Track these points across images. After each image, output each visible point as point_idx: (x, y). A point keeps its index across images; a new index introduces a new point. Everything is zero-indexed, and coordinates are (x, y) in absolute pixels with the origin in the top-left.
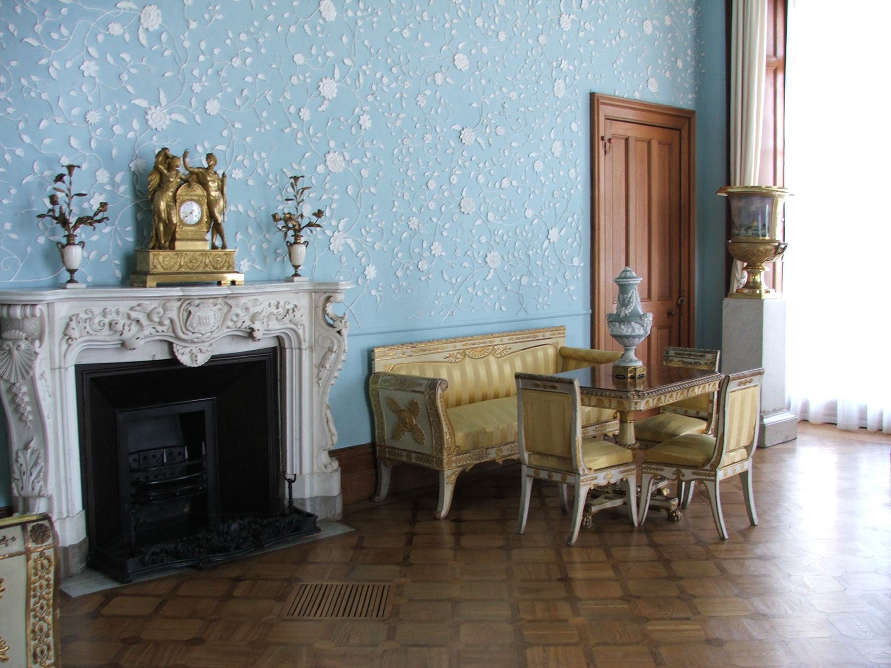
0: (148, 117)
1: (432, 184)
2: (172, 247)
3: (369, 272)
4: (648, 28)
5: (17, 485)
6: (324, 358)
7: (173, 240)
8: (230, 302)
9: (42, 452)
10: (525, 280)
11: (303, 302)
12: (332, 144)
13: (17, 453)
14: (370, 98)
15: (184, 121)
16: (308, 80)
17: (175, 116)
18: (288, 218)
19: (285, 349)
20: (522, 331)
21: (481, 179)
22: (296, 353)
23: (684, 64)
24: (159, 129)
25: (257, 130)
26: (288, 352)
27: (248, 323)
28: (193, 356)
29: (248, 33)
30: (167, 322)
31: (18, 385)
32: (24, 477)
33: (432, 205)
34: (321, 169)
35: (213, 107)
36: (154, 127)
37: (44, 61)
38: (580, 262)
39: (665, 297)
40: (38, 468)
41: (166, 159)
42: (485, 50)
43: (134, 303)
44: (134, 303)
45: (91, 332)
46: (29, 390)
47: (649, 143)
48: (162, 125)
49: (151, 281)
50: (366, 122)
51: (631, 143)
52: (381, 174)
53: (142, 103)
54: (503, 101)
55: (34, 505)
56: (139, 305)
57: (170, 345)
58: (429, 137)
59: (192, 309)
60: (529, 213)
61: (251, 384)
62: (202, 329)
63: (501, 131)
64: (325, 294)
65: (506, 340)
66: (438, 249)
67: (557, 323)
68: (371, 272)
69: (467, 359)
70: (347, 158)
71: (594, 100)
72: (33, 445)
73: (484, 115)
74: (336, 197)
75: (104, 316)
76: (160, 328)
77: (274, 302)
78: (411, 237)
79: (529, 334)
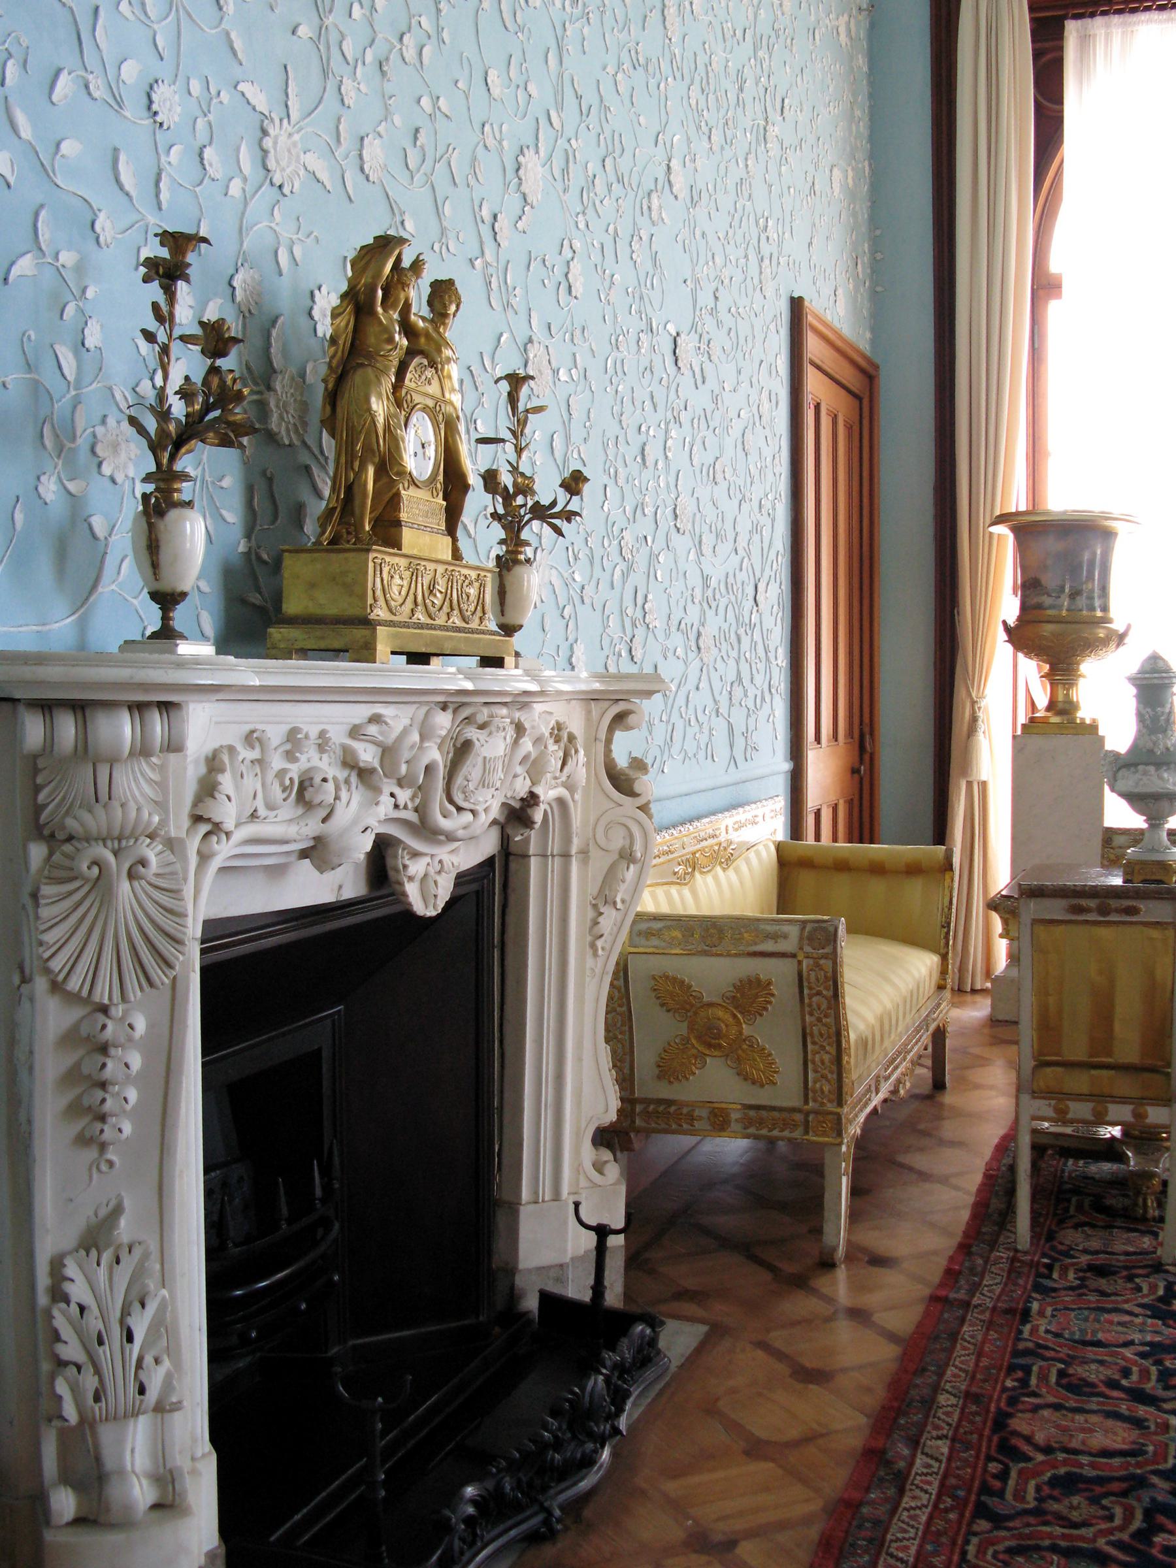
0: (268, 143)
3: (578, 659)
5: (75, 1389)
9: (153, 1246)
13: (57, 1265)
15: (323, 176)
16: (505, 143)
17: (314, 161)
19: (526, 856)
24: (286, 190)
25: (436, 247)
26: (534, 863)
31: (118, 1011)
32: (103, 1353)
36: (277, 180)
38: (782, 659)
39: (850, 733)
40: (152, 1307)
43: (359, 713)
44: (359, 713)
45: (262, 812)
46: (151, 1026)
49: (384, 642)
52: (592, 416)
54: (714, 285)
55: (121, 1442)
56: (375, 719)
59: (472, 733)
69: (697, 874)
70: (554, 365)
72: (125, 1229)
73: (698, 313)
75: (290, 756)
76: (404, 796)
78: (625, 576)
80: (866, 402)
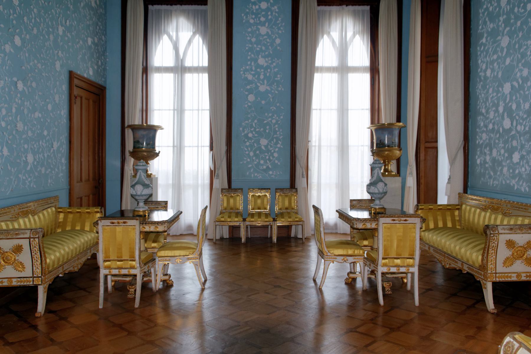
4: (90, 40)
51: (84, 100)
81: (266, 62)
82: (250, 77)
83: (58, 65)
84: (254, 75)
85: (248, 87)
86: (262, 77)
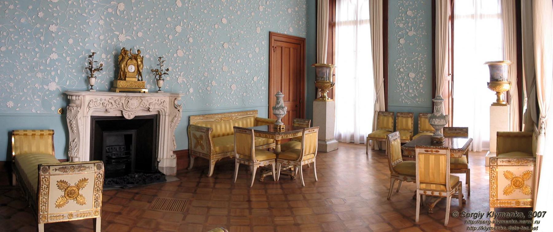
1: (213, 61)
2: (125, 80)
4: (290, 11)
6: (173, 119)
7: (126, 77)
8: (143, 99)
10: (245, 94)
11: (167, 99)
12: (179, 47)
14: (192, 33)
18: (157, 71)
20: (242, 112)
21: (230, 60)
22: (164, 116)
23: (303, 23)
27: (148, 106)
28: (129, 116)
29: (152, 11)
30: (121, 104)
33: (213, 68)
34: (175, 55)
35: (140, 34)
37: (87, 21)
38: (265, 88)
39: (294, 101)
41: (124, 51)
42: (233, 17)
43: (110, 97)
44: (110, 97)
47: (289, 49)
48: (123, 40)
49: (117, 90)
50: (191, 40)
53: (117, 33)
57: (122, 111)
58: (212, 46)
60: (247, 72)
61: (147, 126)
62: (132, 107)
63: (237, 44)
64: (174, 96)
65: (236, 114)
66: (214, 83)
67: (256, 109)
68: (191, 90)
71: (270, 34)
74: (180, 65)
77: (157, 99)
79: (245, 113)
80: (302, 45)
81: (414, 14)
82: (401, 26)
83: (259, 30)
84: (404, 24)
85: (400, 33)
86: (410, 25)
